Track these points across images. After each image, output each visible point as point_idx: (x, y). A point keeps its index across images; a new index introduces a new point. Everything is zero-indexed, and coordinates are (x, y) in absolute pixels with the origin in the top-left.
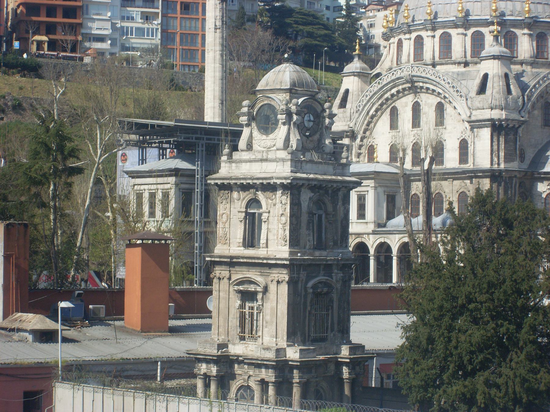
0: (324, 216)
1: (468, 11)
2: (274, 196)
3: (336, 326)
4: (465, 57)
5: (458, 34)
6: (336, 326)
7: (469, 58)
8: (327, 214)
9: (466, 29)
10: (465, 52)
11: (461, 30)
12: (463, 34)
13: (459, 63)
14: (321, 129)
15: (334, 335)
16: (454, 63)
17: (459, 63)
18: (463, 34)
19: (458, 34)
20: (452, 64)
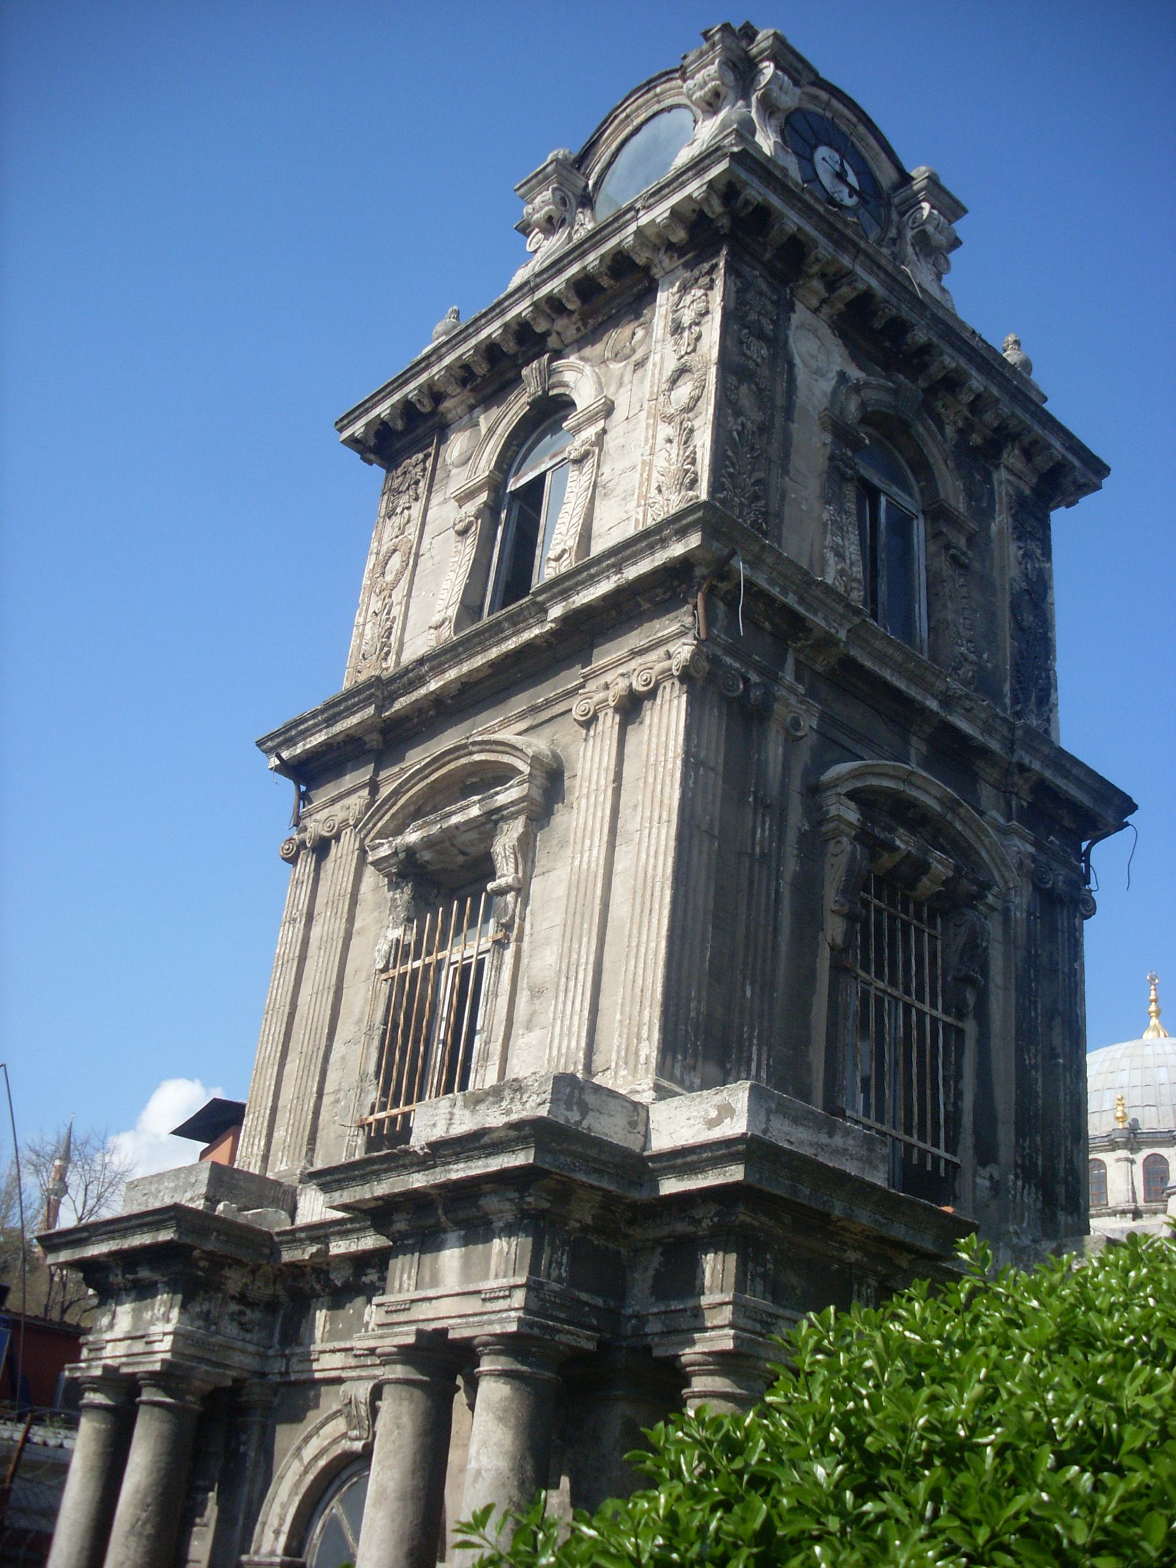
0: (920, 529)
1: (1135, 1121)
2: (640, 333)
3: (1005, 1136)
4: (1135, 1200)
5: (1118, 1160)
6: (1005, 1136)
7: (1141, 1203)
8: (937, 513)
9: (1133, 1150)
10: (1134, 1193)
11: (1123, 1153)
12: (1127, 1160)
13: (1124, 1212)
14: (894, 241)
15: (996, 1187)
16: (1114, 1213)
17: (1124, 1212)
18: (1127, 1160)
19: (1118, 1160)
20: (1109, 1215)
